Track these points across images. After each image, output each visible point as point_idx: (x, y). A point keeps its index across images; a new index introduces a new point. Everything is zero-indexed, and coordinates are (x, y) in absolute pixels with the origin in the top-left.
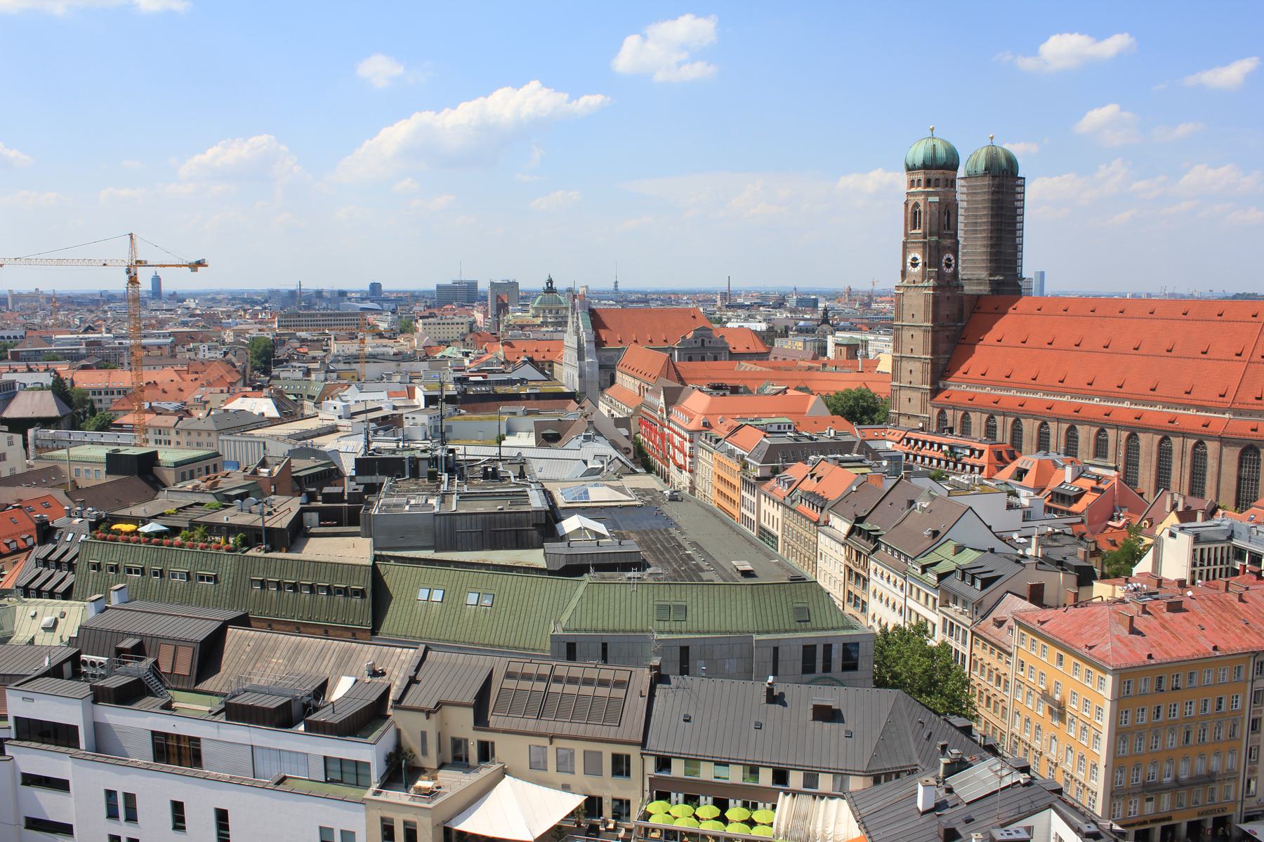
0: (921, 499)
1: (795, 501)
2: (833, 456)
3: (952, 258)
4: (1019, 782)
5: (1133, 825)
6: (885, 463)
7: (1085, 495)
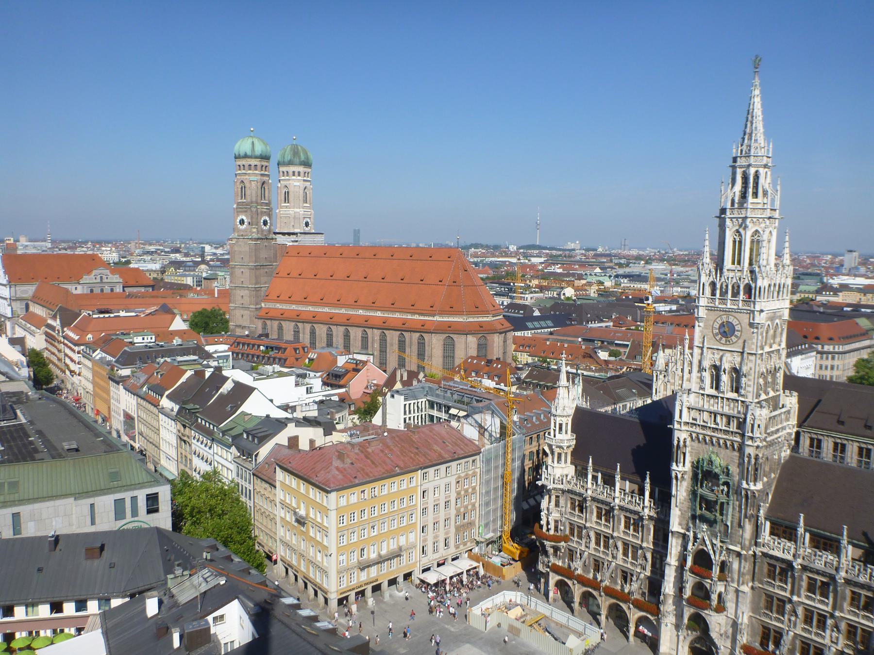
5: (353, 589)
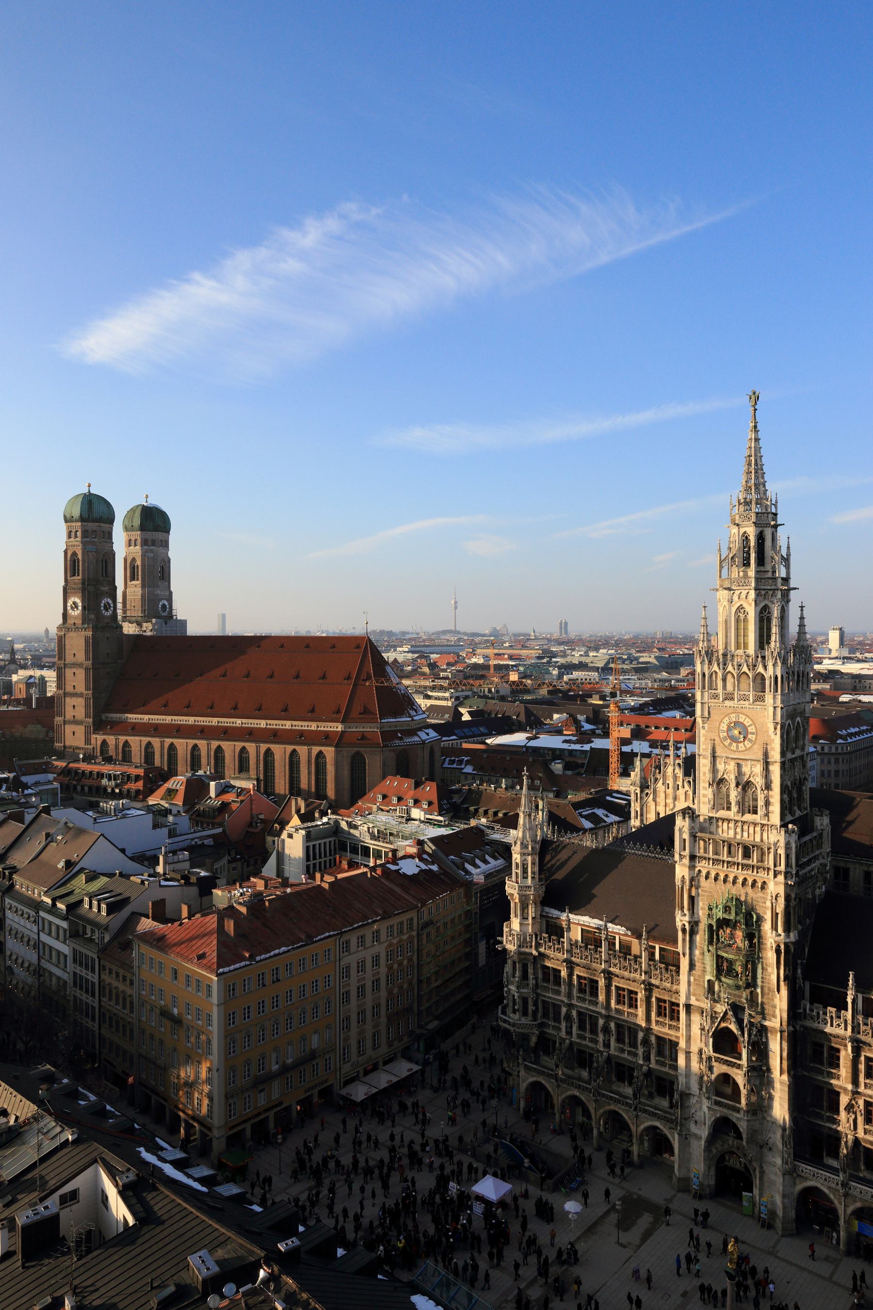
3: (110, 602)
5: (248, 1120)
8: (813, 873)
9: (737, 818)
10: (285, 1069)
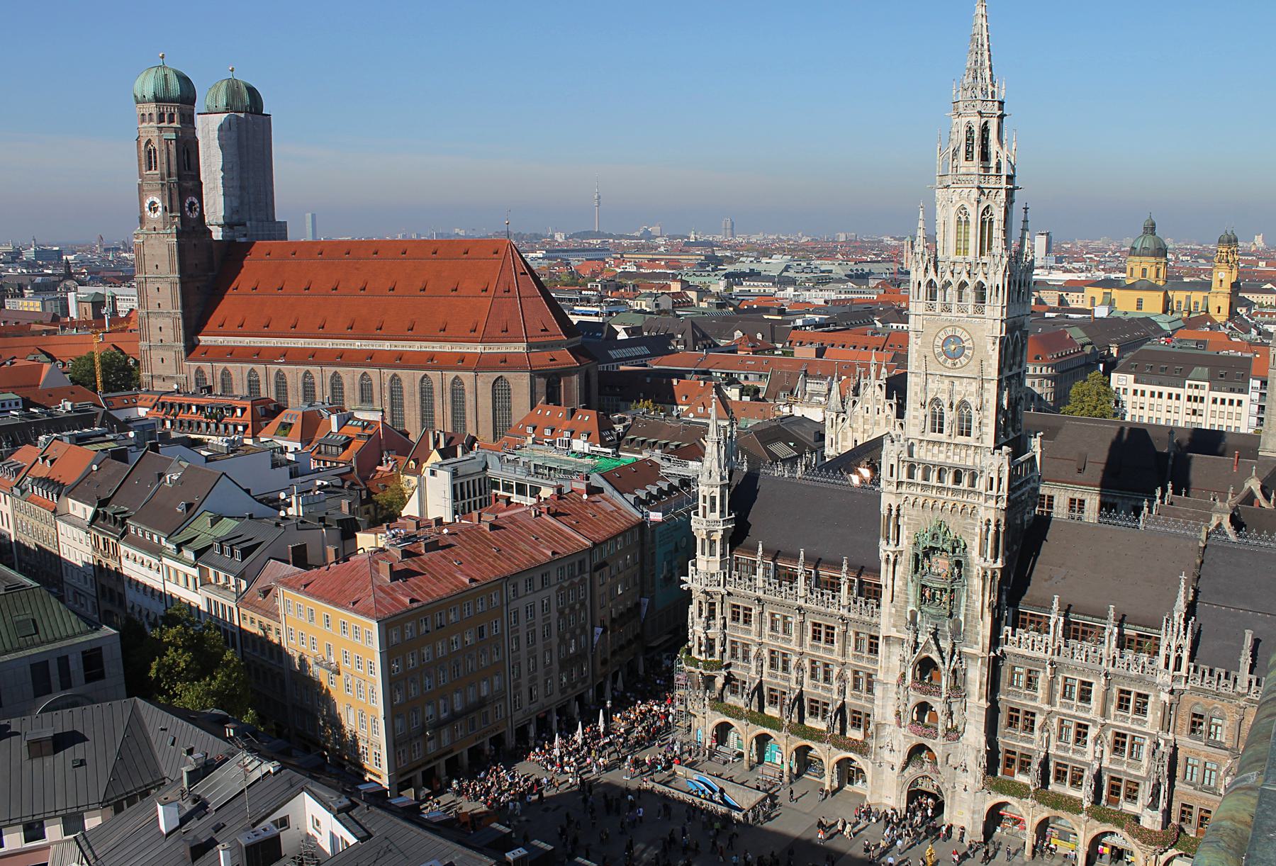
0: (171, 471)
1: (25, 490)
2: (68, 433)
3: (196, 201)
4: (269, 772)
5: (419, 767)
6: (132, 434)
7: (353, 443)
8: (1023, 498)
9: (949, 441)
10: (454, 717)
